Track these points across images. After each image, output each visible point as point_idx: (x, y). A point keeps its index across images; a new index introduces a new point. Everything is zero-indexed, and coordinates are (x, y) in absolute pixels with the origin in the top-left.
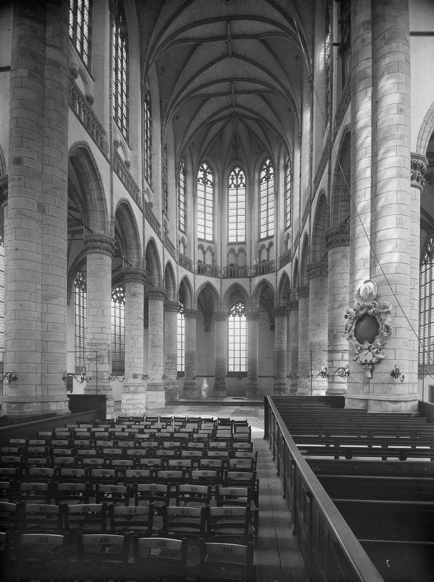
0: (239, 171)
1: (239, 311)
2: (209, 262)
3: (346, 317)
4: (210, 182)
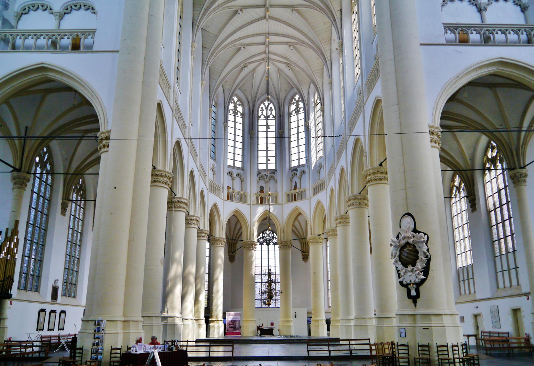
0: (269, 104)
1: (267, 240)
2: (237, 187)
3: (391, 245)
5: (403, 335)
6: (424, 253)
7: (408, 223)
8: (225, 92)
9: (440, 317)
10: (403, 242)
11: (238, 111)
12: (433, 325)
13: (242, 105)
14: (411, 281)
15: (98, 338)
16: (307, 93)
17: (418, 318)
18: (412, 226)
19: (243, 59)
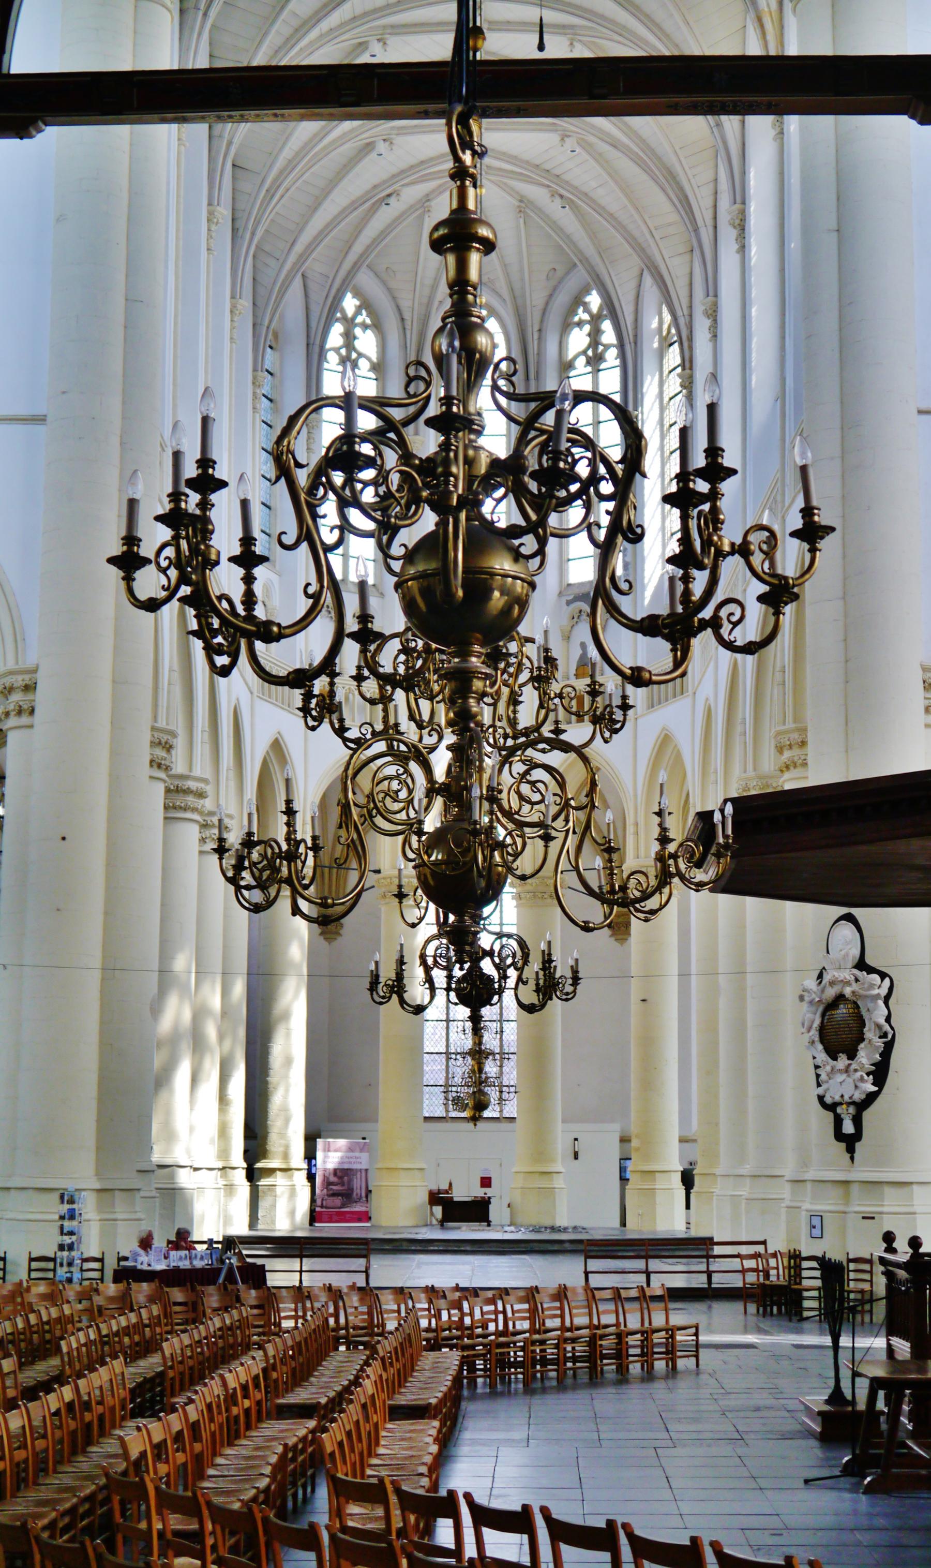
4: (369, 359)
5: (817, 1232)
6: (879, 1027)
7: (847, 943)
8: (312, 285)
9: (906, 1189)
10: (831, 993)
11: (360, 355)
12: (885, 1209)
13: (377, 326)
14: (842, 1096)
15: (71, 1233)
16: (631, 297)
17: (855, 1188)
18: (856, 952)
19: (385, 176)
